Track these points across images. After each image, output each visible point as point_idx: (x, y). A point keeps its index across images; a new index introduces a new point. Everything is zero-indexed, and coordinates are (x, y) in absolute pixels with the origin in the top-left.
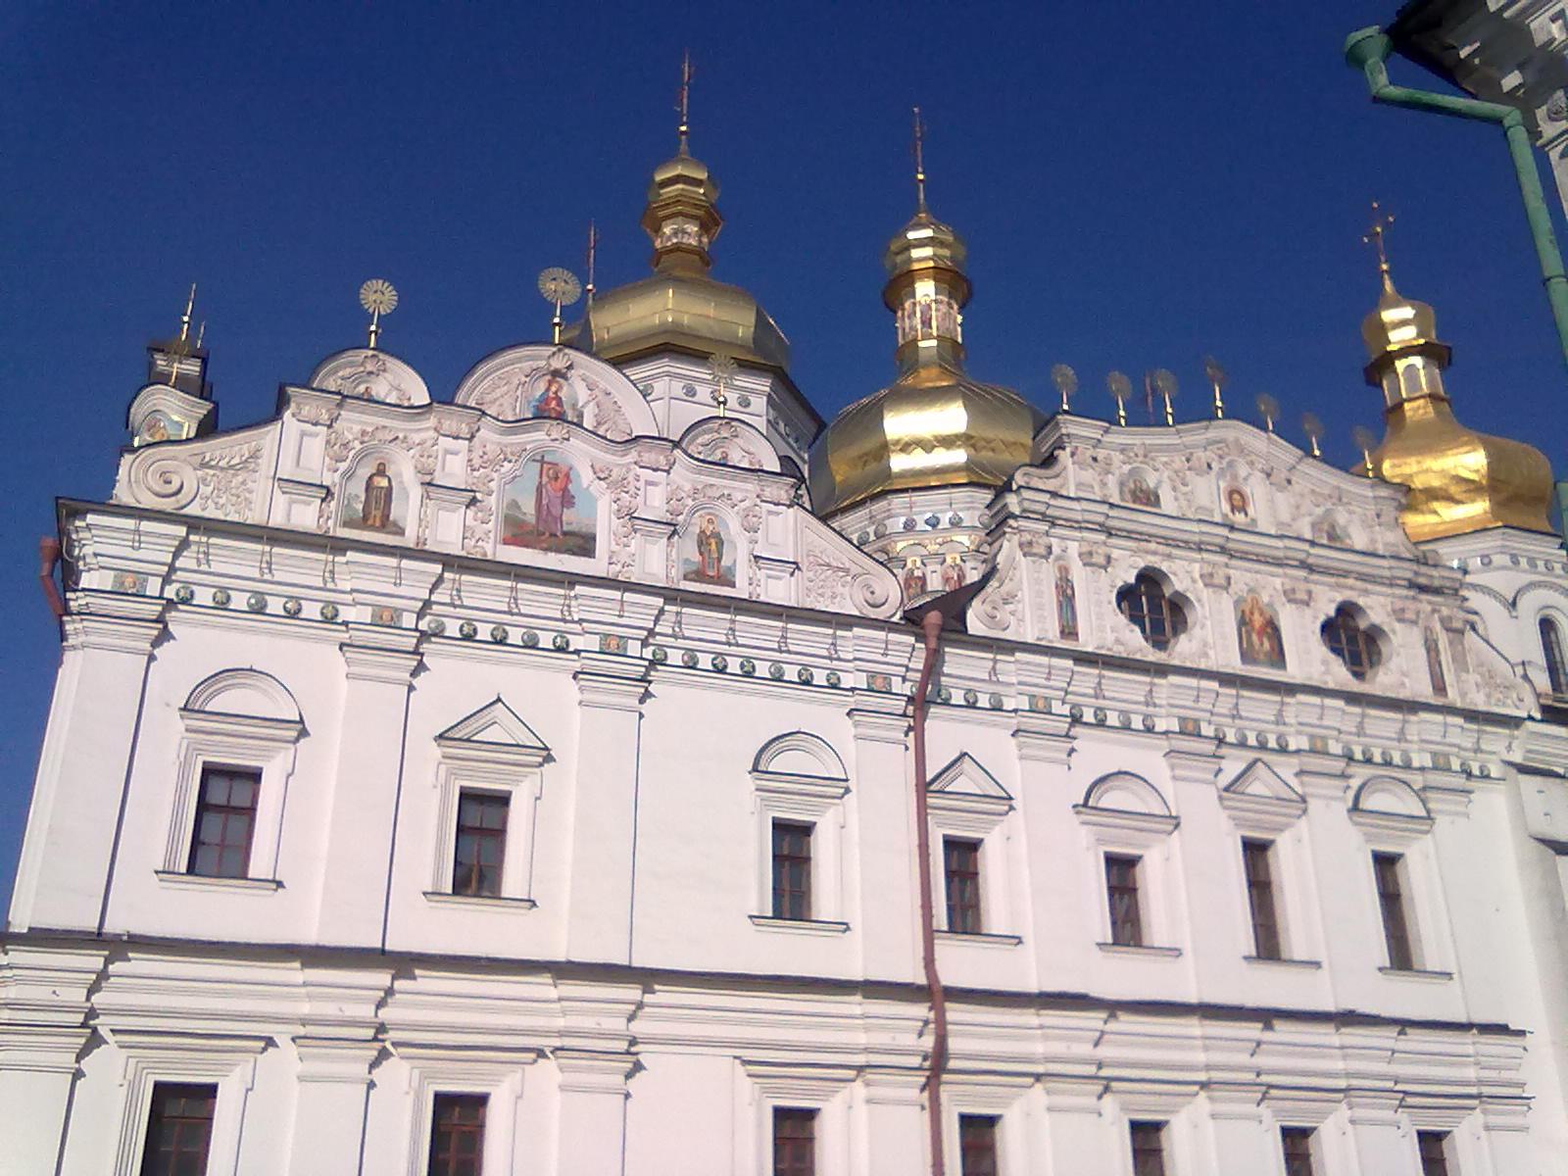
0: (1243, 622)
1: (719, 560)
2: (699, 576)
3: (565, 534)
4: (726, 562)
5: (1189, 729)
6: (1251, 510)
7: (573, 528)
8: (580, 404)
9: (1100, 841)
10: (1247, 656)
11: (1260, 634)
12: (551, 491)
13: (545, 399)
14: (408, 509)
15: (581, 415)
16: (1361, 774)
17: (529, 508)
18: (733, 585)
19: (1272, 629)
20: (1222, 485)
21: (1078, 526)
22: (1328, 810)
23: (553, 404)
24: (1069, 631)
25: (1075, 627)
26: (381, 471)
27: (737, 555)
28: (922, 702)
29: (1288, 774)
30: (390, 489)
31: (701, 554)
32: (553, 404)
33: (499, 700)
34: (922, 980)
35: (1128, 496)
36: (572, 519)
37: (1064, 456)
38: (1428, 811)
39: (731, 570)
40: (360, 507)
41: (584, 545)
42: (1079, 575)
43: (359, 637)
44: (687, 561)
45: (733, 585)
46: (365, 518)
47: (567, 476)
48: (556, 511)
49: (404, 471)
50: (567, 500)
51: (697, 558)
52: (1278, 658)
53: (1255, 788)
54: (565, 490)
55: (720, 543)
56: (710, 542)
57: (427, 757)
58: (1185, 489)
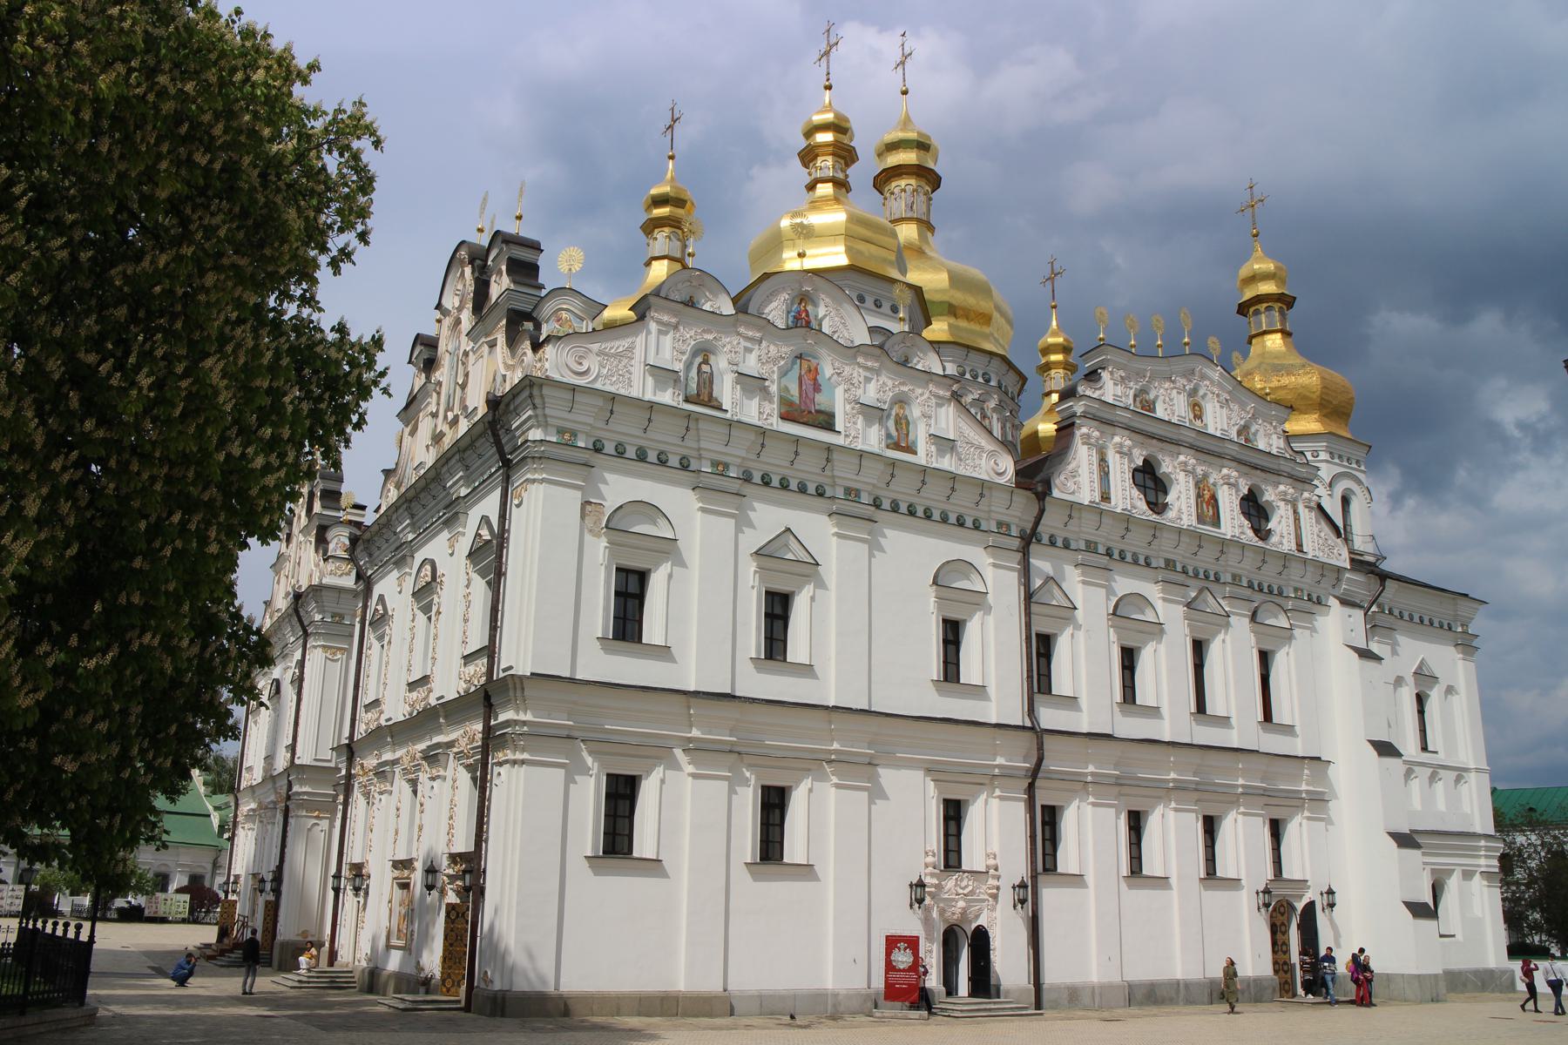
0: (1199, 496)
1: (907, 435)
2: (897, 446)
3: (818, 412)
4: (911, 437)
7: (822, 408)
8: (820, 316)
10: (1200, 519)
11: (1208, 505)
12: (808, 382)
13: (799, 313)
14: (727, 391)
15: (820, 325)
16: (1259, 597)
18: (915, 453)
19: (1214, 500)
23: (803, 315)
24: (1106, 497)
25: (1109, 493)
26: (706, 362)
28: (1029, 539)
30: (712, 374)
31: (897, 430)
32: (803, 315)
34: (1028, 724)
35: (1138, 404)
36: (821, 400)
37: (1105, 375)
39: (914, 443)
40: (695, 386)
41: (826, 421)
43: (705, 480)
45: (915, 453)
46: (698, 395)
47: (816, 369)
48: (811, 395)
49: (720, 363)
50: (817, 388)
52: (1216, 521)
54: (815, 379)
55: (908, 423)
56: (903, 423)
57: (749, 568)
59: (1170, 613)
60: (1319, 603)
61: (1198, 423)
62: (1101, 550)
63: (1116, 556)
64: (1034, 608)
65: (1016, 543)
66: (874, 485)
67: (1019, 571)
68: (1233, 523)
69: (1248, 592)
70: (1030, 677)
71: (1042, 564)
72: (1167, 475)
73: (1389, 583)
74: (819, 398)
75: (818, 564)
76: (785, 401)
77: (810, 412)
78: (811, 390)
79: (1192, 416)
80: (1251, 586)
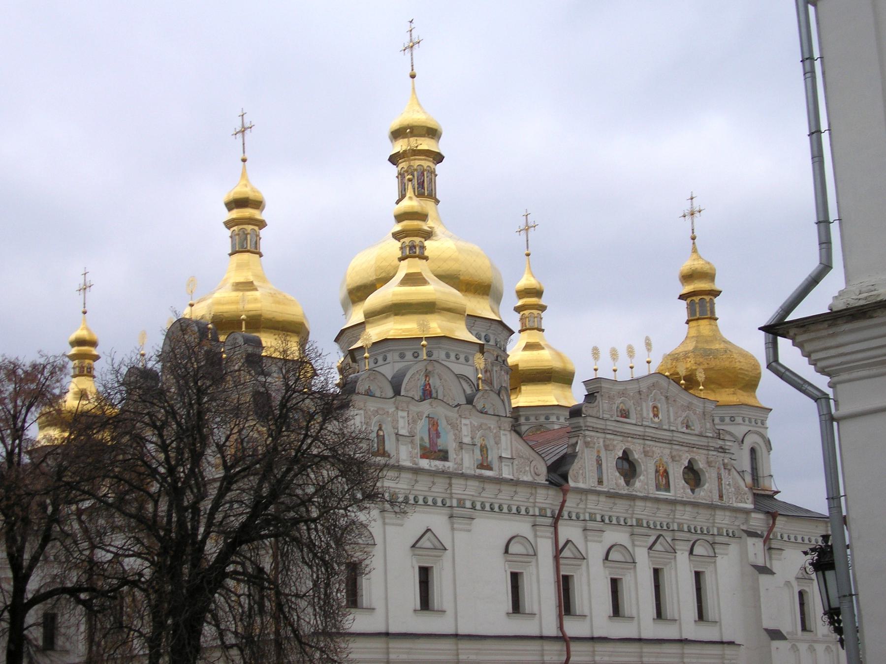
0: (657, 471)
2: (481, 466)
4: (489, 459)
5: (639, 524)
6: (660, 416)
9: (610, 574)
10: (658, 488)
13: (425, 386)
16: (695, 537)
17: (427, 440)
19: (666, 473)
20: (651, 404)
21: (604, 431)
22: (682, 557)
24: (600, 482)
27: (492, 456)
29: (669, 540)
33: (428, 530)
35: (619, 414)
38: (715, 553)
42: (603, 454)
44: (477, 459)
45: (491, 469)
50: (438, 435)
51: (480, 458)
52: (667, 488)
53: (658, 547)
56: (484, 449)
58: (639, 409)
59: (641, 554)
60: (734, 536)
61: (656, 420)
62: (599, 518)
63: (607, 521)
64: (562, 561)
65: (550, 521)
66: (473, 495)
67: (552, 538)
68: (679, 488)
69: (688, 535)
70: (560, 606)
71: (568, 531)
72: (635, 459)
73: (779, 518)
74: (439, 441)
75: (445, 549)
76: (423, 448)
77: (435, 452)
78: (435, 436)
79: (651, 415)
80: (689, 531)
